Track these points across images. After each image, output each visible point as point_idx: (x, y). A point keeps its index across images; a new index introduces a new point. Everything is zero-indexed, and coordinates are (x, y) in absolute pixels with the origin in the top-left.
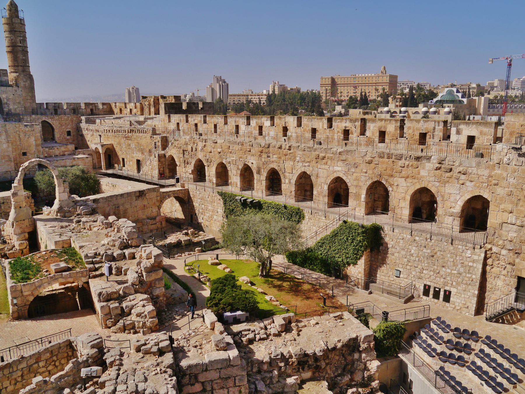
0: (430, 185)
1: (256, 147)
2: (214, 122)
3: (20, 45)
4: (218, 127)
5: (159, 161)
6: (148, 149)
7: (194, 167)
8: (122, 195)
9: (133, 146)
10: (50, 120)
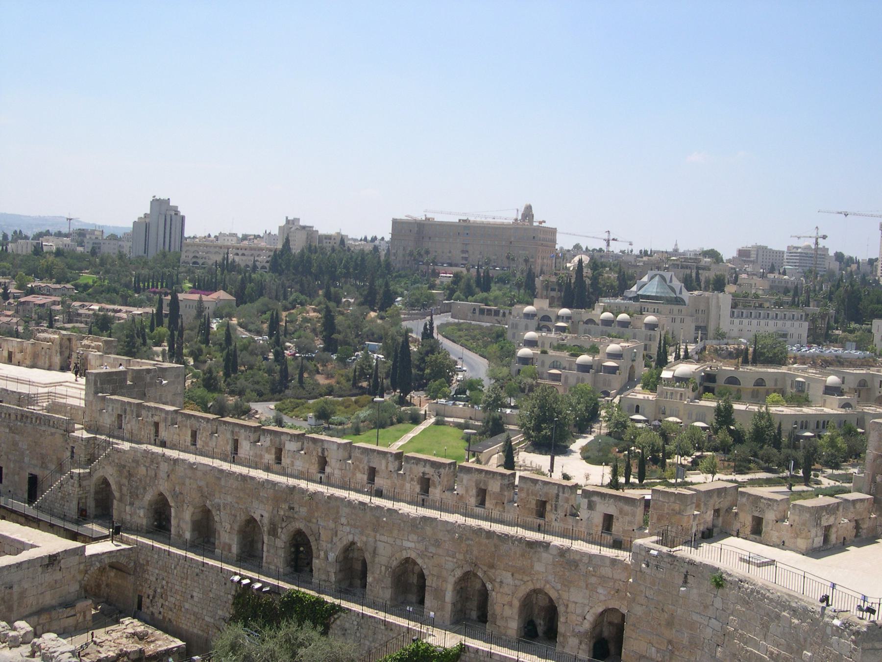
0: (548, 586)
1: (270, 488)
2: (191, 427)
4: (199, 436)
5: (80, 486)
6: (55, 457)
7: (150, 505)
8: (19, 565)
9: (23, 445)
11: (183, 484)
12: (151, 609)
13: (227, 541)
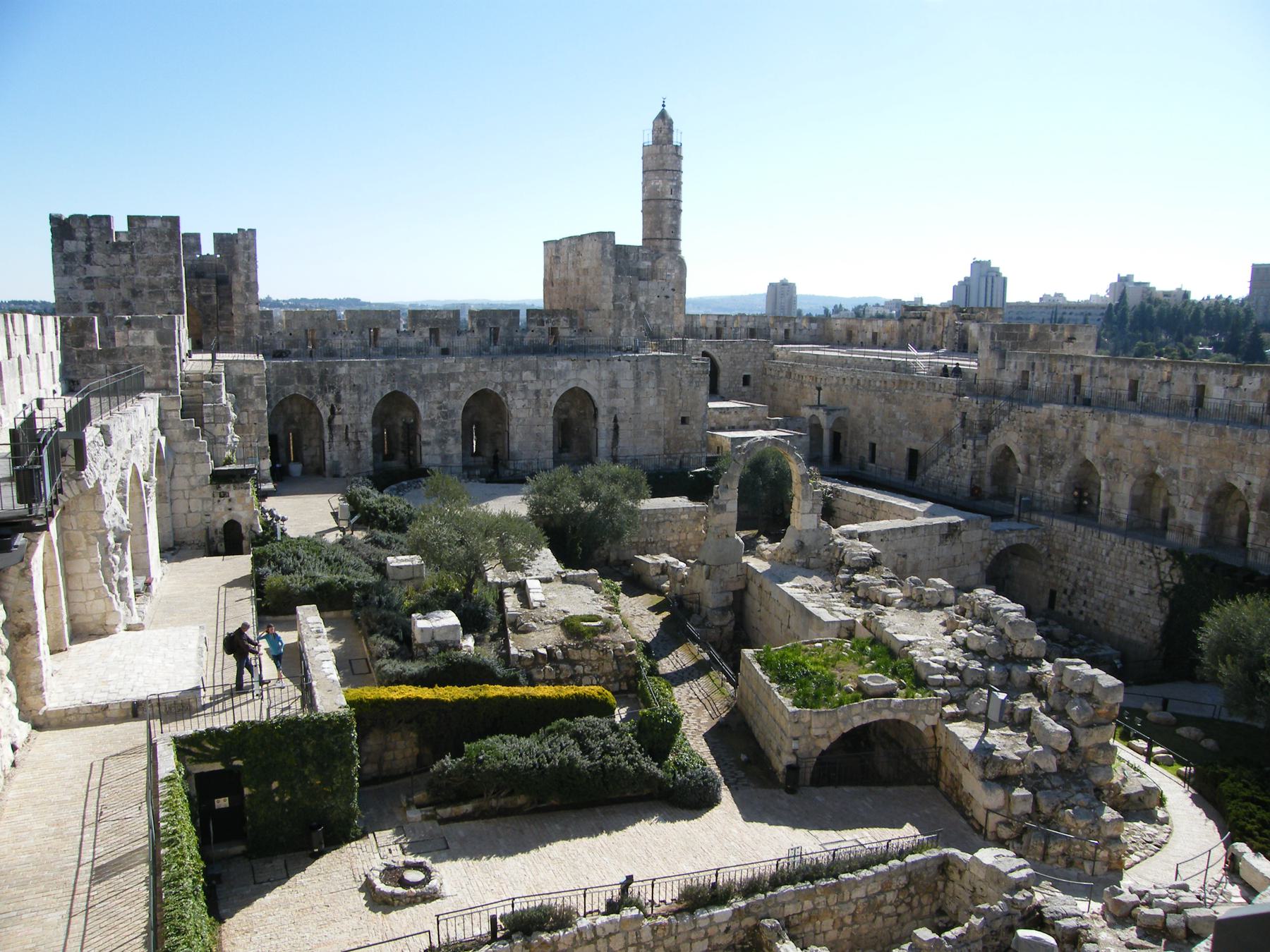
2: (1129, 376)
3: (671, 197)
4: (1141, 387)
5: (975, 457)
6: (941, 428)
7: (1069, 478)
10: (716, 350)
11: (1121, 446)
12: (1068, 607)
13: (1188, 520)
